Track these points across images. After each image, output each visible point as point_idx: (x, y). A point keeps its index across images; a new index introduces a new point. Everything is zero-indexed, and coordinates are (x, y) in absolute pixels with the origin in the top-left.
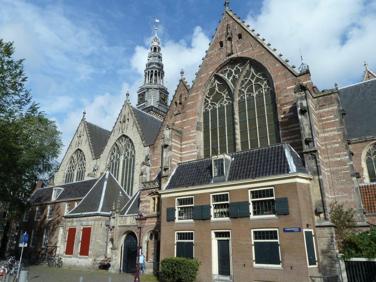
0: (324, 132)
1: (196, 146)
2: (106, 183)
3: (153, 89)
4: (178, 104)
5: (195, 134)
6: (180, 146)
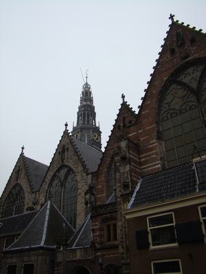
4: (122, 128)
6: (138, 161)
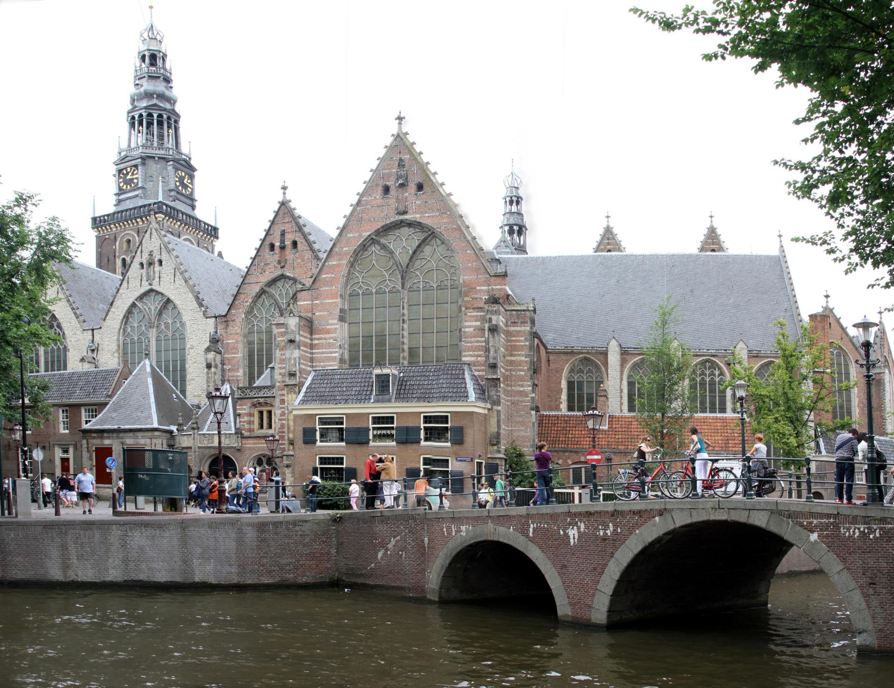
0: (511, 355)
1: (338, 345)
2: (150, 381)
3: (156, 159)
5: (336, 326)
6: (309, 342)
